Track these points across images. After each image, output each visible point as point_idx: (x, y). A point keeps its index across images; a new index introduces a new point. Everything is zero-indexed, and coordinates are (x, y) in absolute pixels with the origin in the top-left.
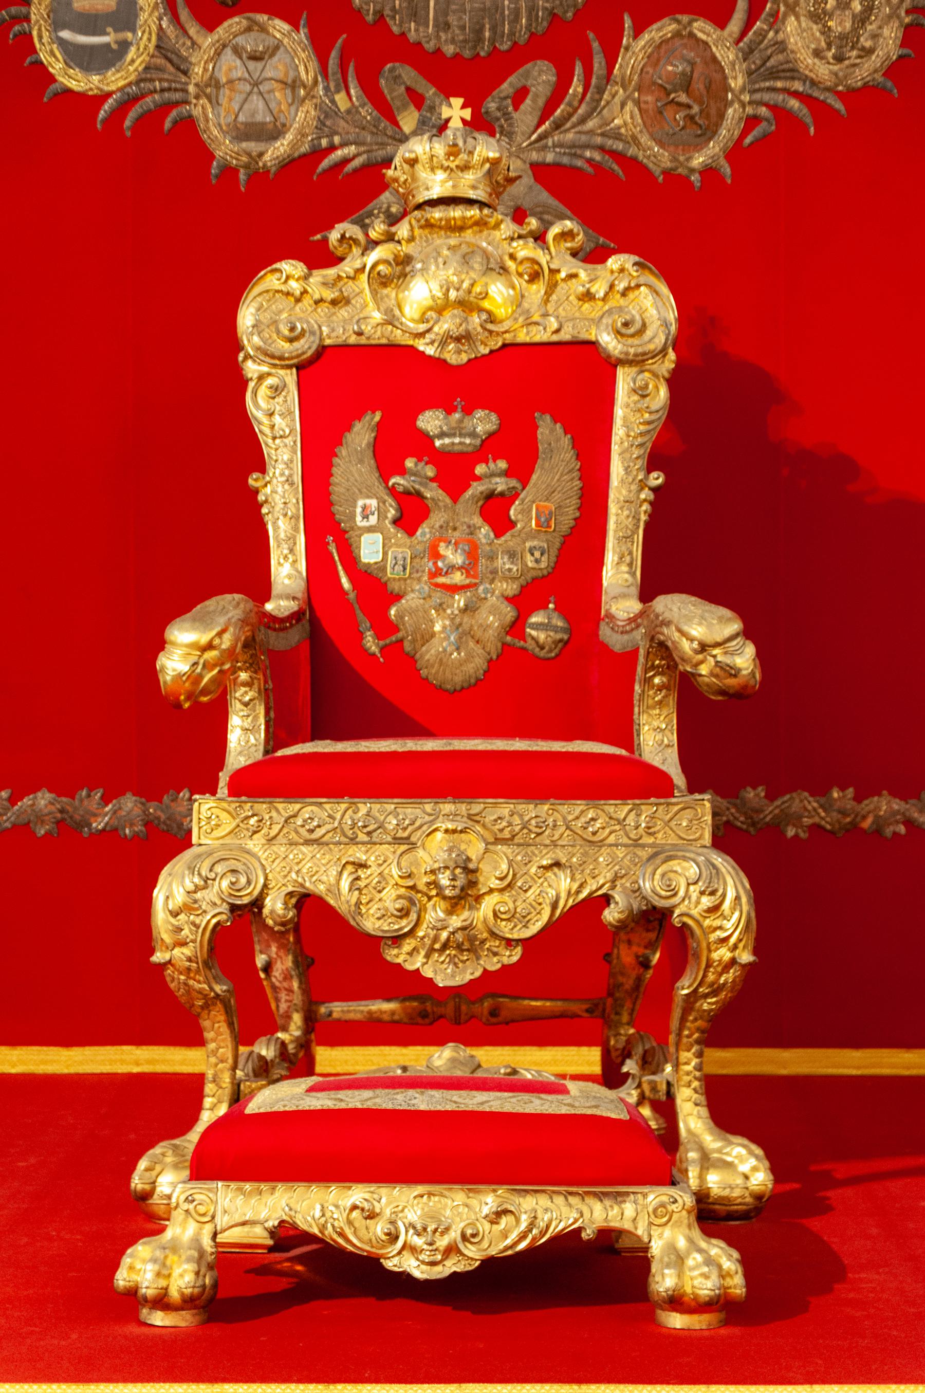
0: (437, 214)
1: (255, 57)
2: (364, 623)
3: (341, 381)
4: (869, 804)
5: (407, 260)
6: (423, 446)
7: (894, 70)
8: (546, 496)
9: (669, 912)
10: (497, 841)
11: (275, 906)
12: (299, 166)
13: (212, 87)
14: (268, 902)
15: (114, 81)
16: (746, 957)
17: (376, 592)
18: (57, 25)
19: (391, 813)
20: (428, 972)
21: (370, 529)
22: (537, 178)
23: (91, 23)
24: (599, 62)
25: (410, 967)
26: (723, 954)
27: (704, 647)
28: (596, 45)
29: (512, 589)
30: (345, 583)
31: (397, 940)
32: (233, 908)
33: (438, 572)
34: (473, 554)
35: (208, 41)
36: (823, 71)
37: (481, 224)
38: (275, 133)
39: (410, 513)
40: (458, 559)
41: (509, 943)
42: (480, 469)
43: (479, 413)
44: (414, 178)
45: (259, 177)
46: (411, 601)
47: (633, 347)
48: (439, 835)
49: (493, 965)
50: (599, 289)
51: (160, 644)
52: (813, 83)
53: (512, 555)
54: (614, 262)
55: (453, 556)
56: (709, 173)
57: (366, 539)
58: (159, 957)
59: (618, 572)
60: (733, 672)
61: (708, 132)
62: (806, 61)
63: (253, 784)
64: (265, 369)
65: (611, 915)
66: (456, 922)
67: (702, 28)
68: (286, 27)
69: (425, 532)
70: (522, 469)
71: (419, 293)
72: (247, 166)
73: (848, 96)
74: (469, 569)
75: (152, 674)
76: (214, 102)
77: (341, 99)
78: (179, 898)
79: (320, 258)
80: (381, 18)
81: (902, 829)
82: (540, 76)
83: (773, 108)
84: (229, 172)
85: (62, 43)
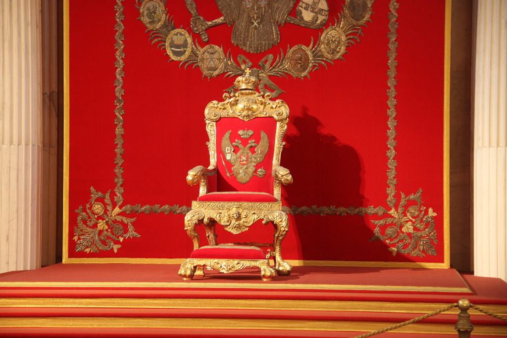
0: (243, 91)
1: (212, 54)
2: (227, 171)
3: (223, 124)
4: (338, 209)
5: (238, 100)
6: (239, 137)
7: (343, 55)
8: (262, 148)
9: (274, 221)
10: (245, 209)
11: (206, 220)
12: (220, 76)
13: (202, 60)
14: (205, 219)
15: (183, 58)
16: (286, 230)
17: (229, 164)
18: (171, 47)
19: (226, 204)
20: (232, 232)
21: (229, 153)
22: (270, 78)
23: (178, 46)
24: (282, 54)
25: (229, 231)
26: (283, 229)
27: (282, 176)
28: (282, 51)
30: (224, 163)
31: (227, 226)
32: (198, 220)
33: (241, 161)
34: (247, 158)
35: (202, 50)
36: (329, 56)
37: (251, 94)
38: (216, 69)
39: (236, 150)
40: (245, 159)
41: (246, 227)
42: (250, 142)
43: (250, 131)
44: (239, 85)
45: (212, 78)
46: (235, 167)
47: (281, 118)
48: (234, 208)
49: (244, 230)
50: (274, 106)
51: (187, 174)
52: (327, 59)
53: (255, 158)
54: (277, 101)
56: (305, 77)
57: (228, 155)
58: (186, 229)
59: (276, 160)
60: (287, 180)
61: (305, 69)
62: (326, 54)
63: (204, 199)
64: (210, 122)
65: (264, 222)
66: (237, 223)
67: (304, 47)
68: (218, 47)
69: (239, 154)
70: (258, 142)
71: (240, 106)
72: (210, 76)
73: (335, 61)
74: (247, 160)
76: (203, 63)
77: (229, 62)
78: (189, 218)
80: (237, 46)
81: (346, 214)
83: (319, 64)
84: (206, 77)
85: (172, 50)
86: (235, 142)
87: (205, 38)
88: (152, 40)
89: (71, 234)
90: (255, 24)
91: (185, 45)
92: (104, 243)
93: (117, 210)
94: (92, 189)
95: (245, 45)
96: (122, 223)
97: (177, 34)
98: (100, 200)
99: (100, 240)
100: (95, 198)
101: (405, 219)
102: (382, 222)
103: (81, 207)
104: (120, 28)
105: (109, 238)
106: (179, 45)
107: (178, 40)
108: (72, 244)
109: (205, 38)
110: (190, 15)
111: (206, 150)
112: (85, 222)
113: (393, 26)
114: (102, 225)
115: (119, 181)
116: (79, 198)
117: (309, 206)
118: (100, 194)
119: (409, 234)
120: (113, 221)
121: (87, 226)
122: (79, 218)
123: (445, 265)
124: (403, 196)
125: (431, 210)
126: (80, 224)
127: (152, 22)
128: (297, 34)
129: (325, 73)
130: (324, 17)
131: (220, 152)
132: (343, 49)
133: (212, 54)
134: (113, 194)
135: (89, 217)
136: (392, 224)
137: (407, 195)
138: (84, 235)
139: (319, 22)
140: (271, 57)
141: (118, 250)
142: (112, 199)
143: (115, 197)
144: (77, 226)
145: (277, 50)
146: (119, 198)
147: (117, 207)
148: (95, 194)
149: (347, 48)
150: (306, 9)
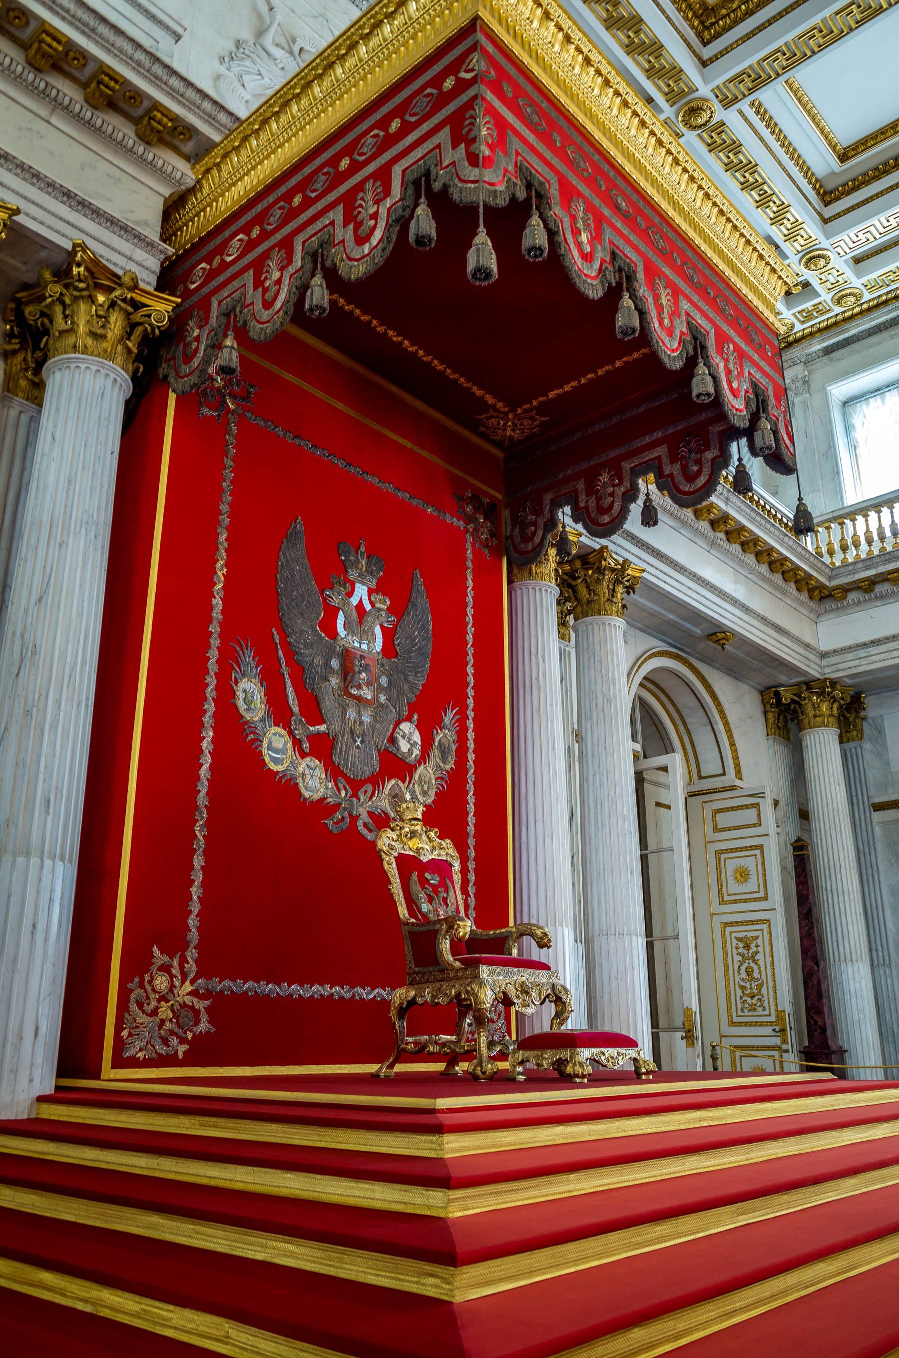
23: (276, 751)
82: (369, 787)
84: (305, 799)
87: (306, 745)
88: (247, 735)
89: (119, 1028)
92: (165, 1042)
93: (187, 987)
95: (347, 768)
96: (192, 1008)
97: (275, 734)
98: (165, 968)
99: (161, 1037)
100: (159, 964)
103: (137, 979)
104: (210, 707)
105: (172, 1033)
109: (306, 745)
110: (292, 713)
111: (391, 896)
112: (140, 1005)
113: (471, 777)
114: (165, 1011)
115: (194, 936)
116: (136, 965)
118: (166, 959)
120: (180, 1005)
121: (144, 1012)
122: (133, 996)
126: (134, 1007)
127: (248, 710)
134: (183, 961)
135: (148, 998)
138: (137, 1027)
139: (413, 756)
141: (185, 1053)
142: (182, 967)
143: (186, 965)
144: (129, 1012)
145: (376, 780)
146: (191, 967)
147: (188, 980)
150: (403, 737)
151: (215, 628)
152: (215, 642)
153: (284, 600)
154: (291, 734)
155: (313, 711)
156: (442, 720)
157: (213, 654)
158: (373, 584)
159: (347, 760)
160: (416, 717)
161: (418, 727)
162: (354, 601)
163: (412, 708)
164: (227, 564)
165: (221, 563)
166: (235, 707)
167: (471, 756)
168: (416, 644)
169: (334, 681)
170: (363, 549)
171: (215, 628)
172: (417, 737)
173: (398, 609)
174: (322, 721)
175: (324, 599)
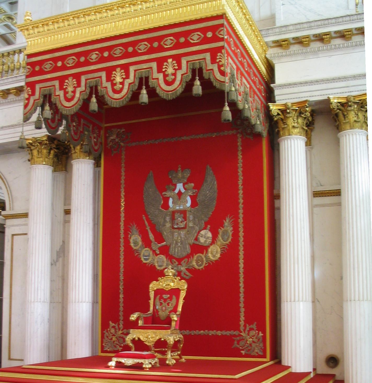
3: (159, 292)
7: (220, 258)
17: (157, 311)
24: (192, 258)
29: (169, 311)
34: (166, 308)
36: (212, 258)
39: (161, 304)
41: (154, 342)
42: (167, 300)
46: (160, 312)
55: (164, 308)
56: (202, 269)
67: (201, 255)
68: (163, 256)
69: (162, 306)
70: (171, 300)
73: (215, 261)
74: (165, 309)
75: (129, 319)
79: (157, 280)
83: (209, 263)
85: (144, 258)
86: (161, 300)
88: (135, 254)
90: (179, 244)
91: (149, 256)
92: (115, 346)
94: (111, 323)
95: (175, 255)
97: (145, 251)
101: (249, 337)
102: (238, 338)
103: (106, 330)
104: (122, 249)
105: (117, 344)
106: (147, 256)
107: (146, 254)
108: (102, 347)
109: (158, 252)
110: (151, 242)
112: (107, 337)
113: (241, 244)
114: (114, 339)
116: (105, 326)
117: (204, 330)
118: (114, 324)
119: (251, 345)
121: (108, 339)
122: (105, 335)
123: (268, 359)
124: (247, 325)
125: (260, 332)
126: (105, 337)
128: (198, 249)
129: (212, 267)
130: (210, 240)
131: (154, 306)
132: (218, 256)
133: (160, 259)
134: (119, 325)
135: (109, 335)
136: (244, 340)
137: (249, 325)
139: (207, 243)
140: (186, 260)
142: (118, 327)
143: (120, 326)
146: (121, 326)
148: (112, 324)
149: (221, 255)
150: (202, 237)
151: (122, 224)
152: (122, 228)
153: (146, 204)
154: (151, 249)
155: (159, 238)
156: (223, 223)
157: (122, 231)
158: (186, 181)
159: (175, 252)
160: (209, 226)
161: (210, 230)
162: (177, 191)
163: (206, 224)
164: (125, 201)
165: (123, 200)
166: (130, 246)
167: (241, 234)
168: (207, 197)
169: (168, 225)
170: (180, 169)
171: (122, 224)
172: (210, 235)
173: (198, 187)
174: (164, 241)
175: (162, 196)
